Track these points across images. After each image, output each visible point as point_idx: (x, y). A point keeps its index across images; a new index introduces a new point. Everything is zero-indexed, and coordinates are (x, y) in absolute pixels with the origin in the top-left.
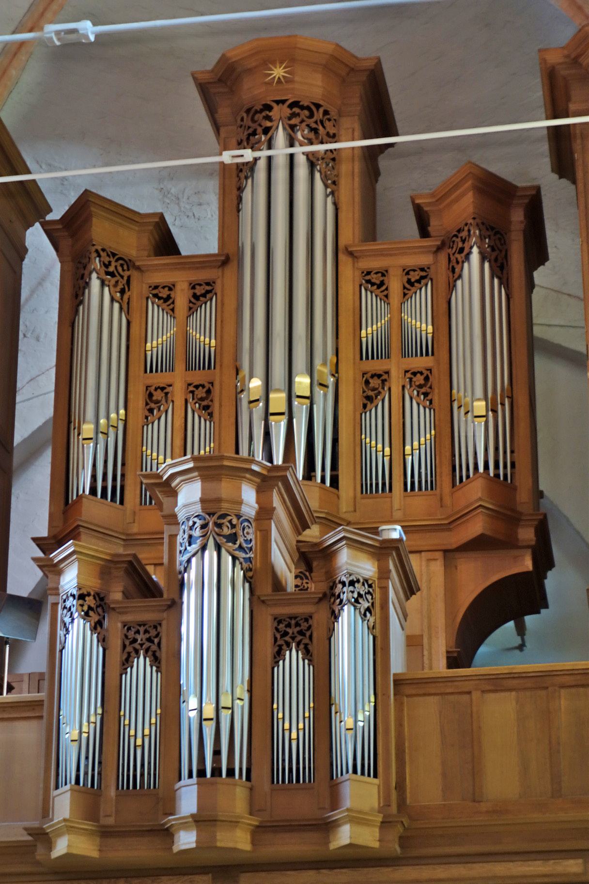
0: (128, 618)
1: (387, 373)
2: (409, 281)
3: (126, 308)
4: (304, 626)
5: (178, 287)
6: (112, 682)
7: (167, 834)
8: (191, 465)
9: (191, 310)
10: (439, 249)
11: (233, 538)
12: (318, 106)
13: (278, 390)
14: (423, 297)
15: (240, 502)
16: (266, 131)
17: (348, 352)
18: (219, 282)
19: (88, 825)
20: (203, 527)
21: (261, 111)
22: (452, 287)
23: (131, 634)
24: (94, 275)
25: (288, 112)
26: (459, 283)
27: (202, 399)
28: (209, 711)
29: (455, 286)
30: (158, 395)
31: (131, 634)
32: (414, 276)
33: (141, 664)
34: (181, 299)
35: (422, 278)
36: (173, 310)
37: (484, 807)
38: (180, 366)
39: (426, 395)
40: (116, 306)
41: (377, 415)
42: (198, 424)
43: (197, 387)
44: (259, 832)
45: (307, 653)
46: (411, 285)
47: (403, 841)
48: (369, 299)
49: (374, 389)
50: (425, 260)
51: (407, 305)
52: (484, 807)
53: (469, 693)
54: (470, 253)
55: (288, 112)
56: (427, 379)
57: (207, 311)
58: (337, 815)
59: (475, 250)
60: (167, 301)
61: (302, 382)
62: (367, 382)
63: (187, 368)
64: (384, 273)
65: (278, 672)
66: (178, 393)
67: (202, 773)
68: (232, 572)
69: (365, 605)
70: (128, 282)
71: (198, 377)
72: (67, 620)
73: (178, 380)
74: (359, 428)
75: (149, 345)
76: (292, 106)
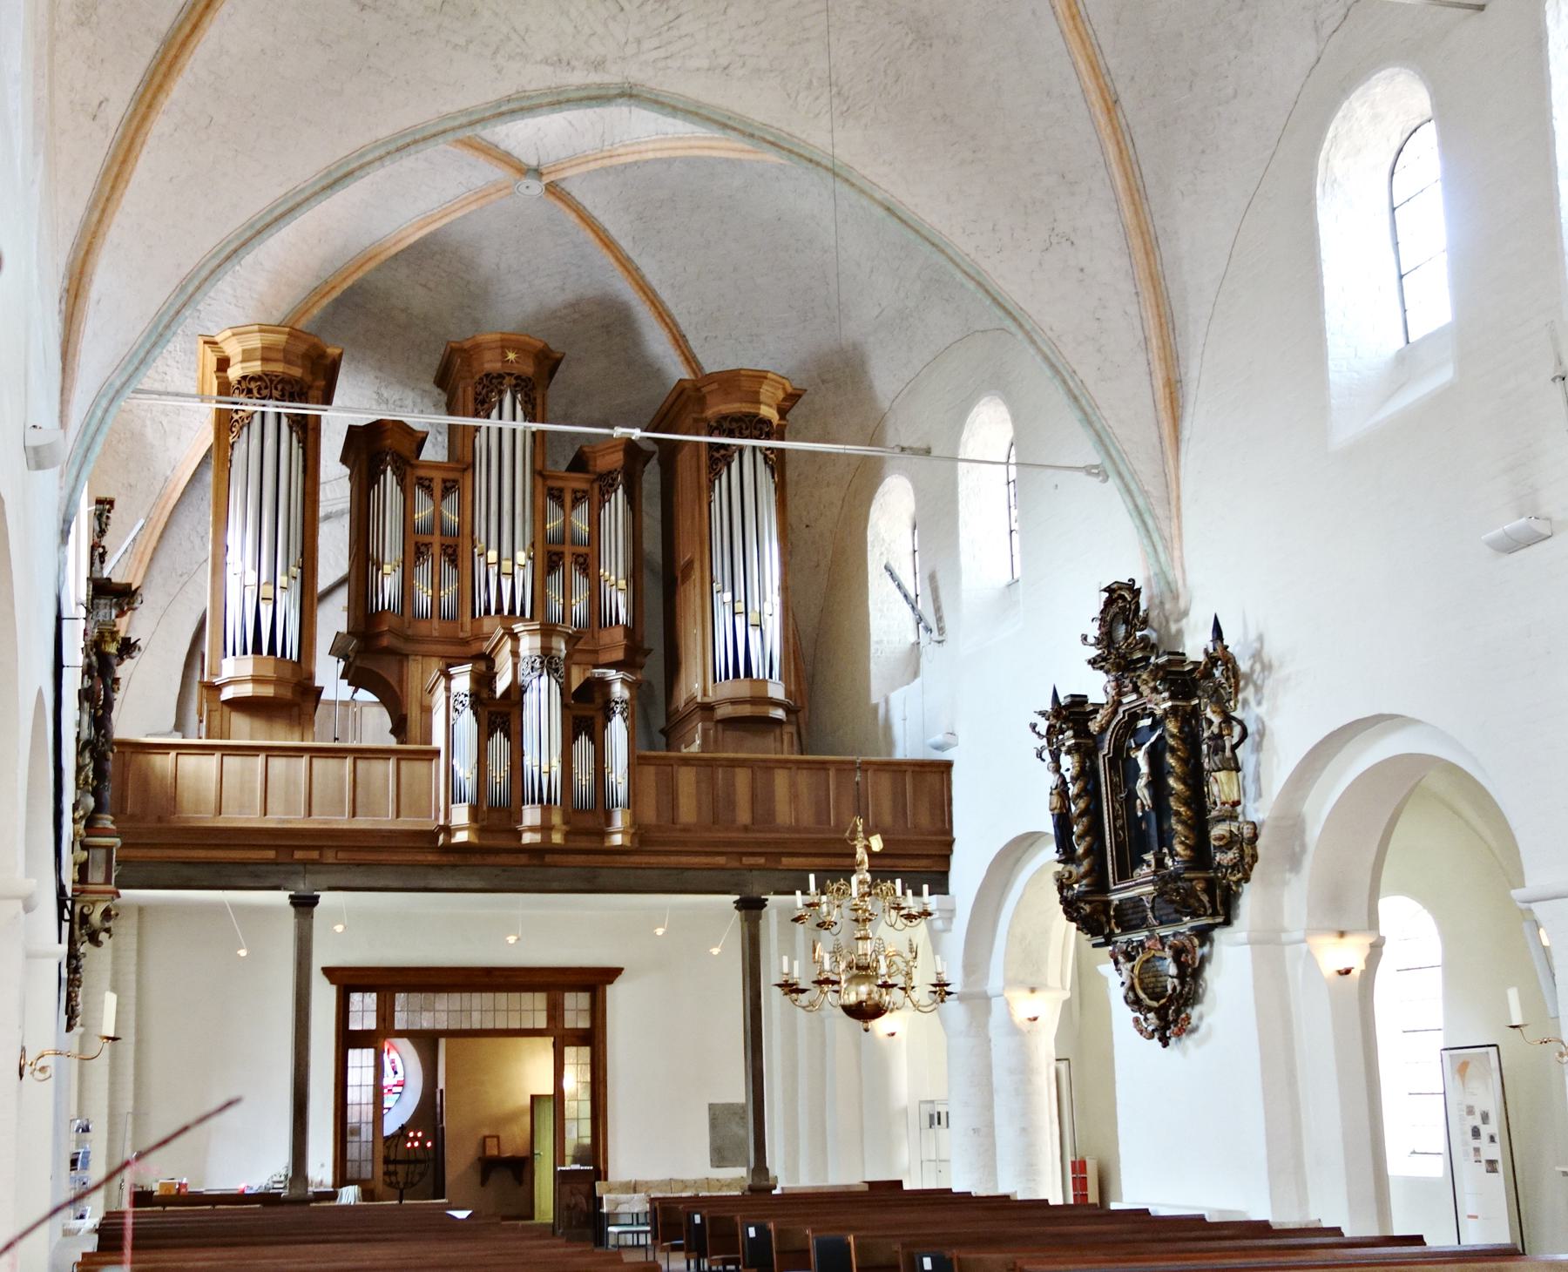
0: (492, 709)
1: (563, 553)
2: (576, 497)
3: (403, 490)
4: (590, 722)
5: (435, 481)
6: (483, 746)
7: (519, 835)
8: (538, 627)
9: (443, 497)
10: (593, 481)
11: (557, 670)
12: (530, 379)
13: (507, 559)
14: (584, 509)
15: (561, 651)
16: (501, 393)
17: (540, 537)
18: (461, 481)
19: (475, 826)
20: (542, 663)
21: (497, 378)
22: (601, 505)
23: (493, 718)
24: (389, 468)
25: (514, 382)
26: (607, 504)
27: (451, 555)
28: (545, 768)
29: (604, 506)
30: (423, 549)
31: (493, 718)
32: (579, 495)
33: (499, 736)
34: (437, 488)
35: (584, 497)
36: (432, 495)
37: (678, 826)
38: (437, 533)
39: (585, 570)
40: (399, 488)
41: (556, 579)
42: (449, 572)
43: (447, 547)
44: (567, 835)
45: (592, 739)
46: (576, 502)
47: (642, 842)
48: (551, 505)
49: (554, 562)
50: (583, 486)
51: (574, 513)
52: (678, 826)
53: (672, 765)
54: (618, 488)
55: (514, 382)
56: (585, 560)
57: (453, 498)
58: (611, 829)
59: (621, 487)
60: (428, 489)
61: (521, 557)
62: (550, 557)
63: (441, 534)
64: (561, 490)
65: (575, 747)
66: (436, 549)
67: (541, 800)
68: (555, 689)
69: (625, 714)
70: (405, 474)
71: (449, 541)
72: (459, 707)
73: (436, 540)
74: (544, 585)
75: (416, 516)
76: (517, 378)
